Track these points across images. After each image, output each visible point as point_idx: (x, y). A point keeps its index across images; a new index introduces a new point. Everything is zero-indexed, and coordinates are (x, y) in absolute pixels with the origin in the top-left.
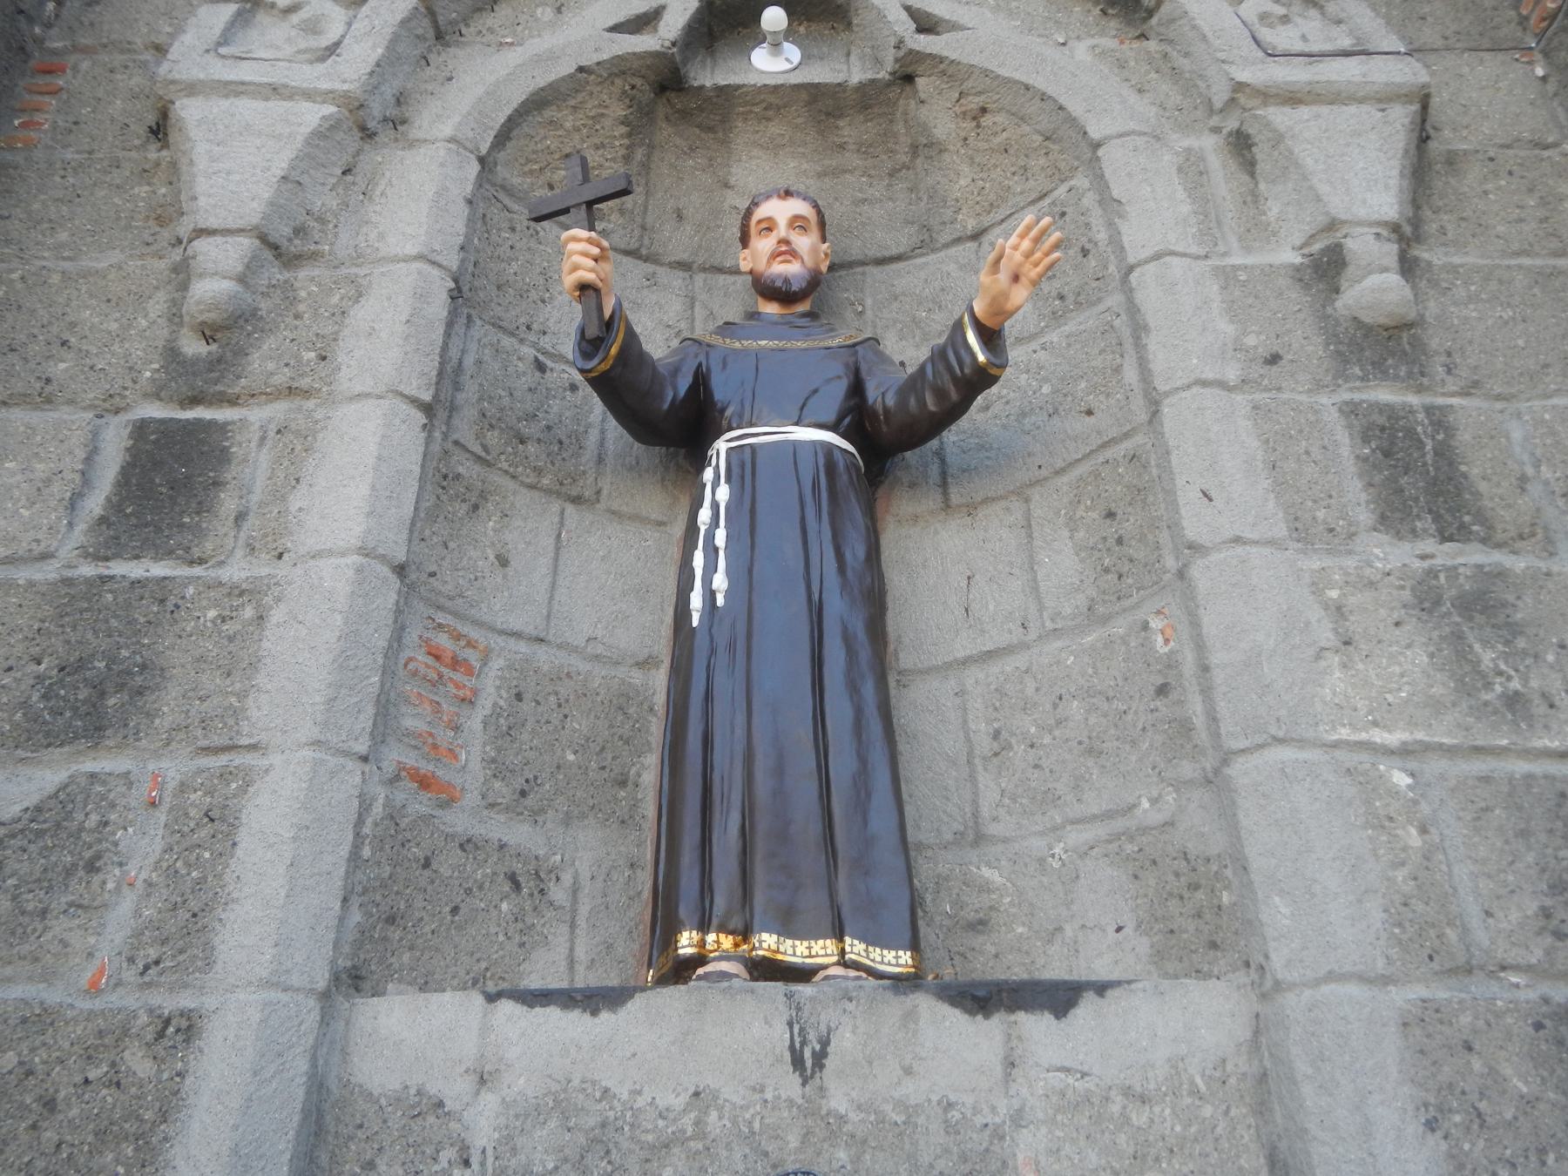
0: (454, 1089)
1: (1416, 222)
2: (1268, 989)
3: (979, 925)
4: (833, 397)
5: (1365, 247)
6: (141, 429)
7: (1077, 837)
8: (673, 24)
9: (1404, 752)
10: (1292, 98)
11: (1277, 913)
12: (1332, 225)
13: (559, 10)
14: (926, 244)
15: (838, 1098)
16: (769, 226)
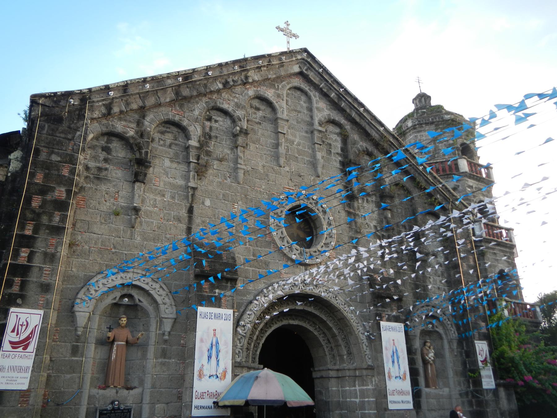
0: (96, 394)
1: (171, 330)
2: (143, 387)
3: (128, 381)
4: (126, 339)
5: (166, 333)
6: (73, 345)
7: (136, 376)
8: (118, 299)
9: (156, 375)
10: (166, 318)
11: (146, 385)
12: (165, 331)
13: (107, 296)
14: (135, 318)
15: (118, 395)
16: (122, 321)
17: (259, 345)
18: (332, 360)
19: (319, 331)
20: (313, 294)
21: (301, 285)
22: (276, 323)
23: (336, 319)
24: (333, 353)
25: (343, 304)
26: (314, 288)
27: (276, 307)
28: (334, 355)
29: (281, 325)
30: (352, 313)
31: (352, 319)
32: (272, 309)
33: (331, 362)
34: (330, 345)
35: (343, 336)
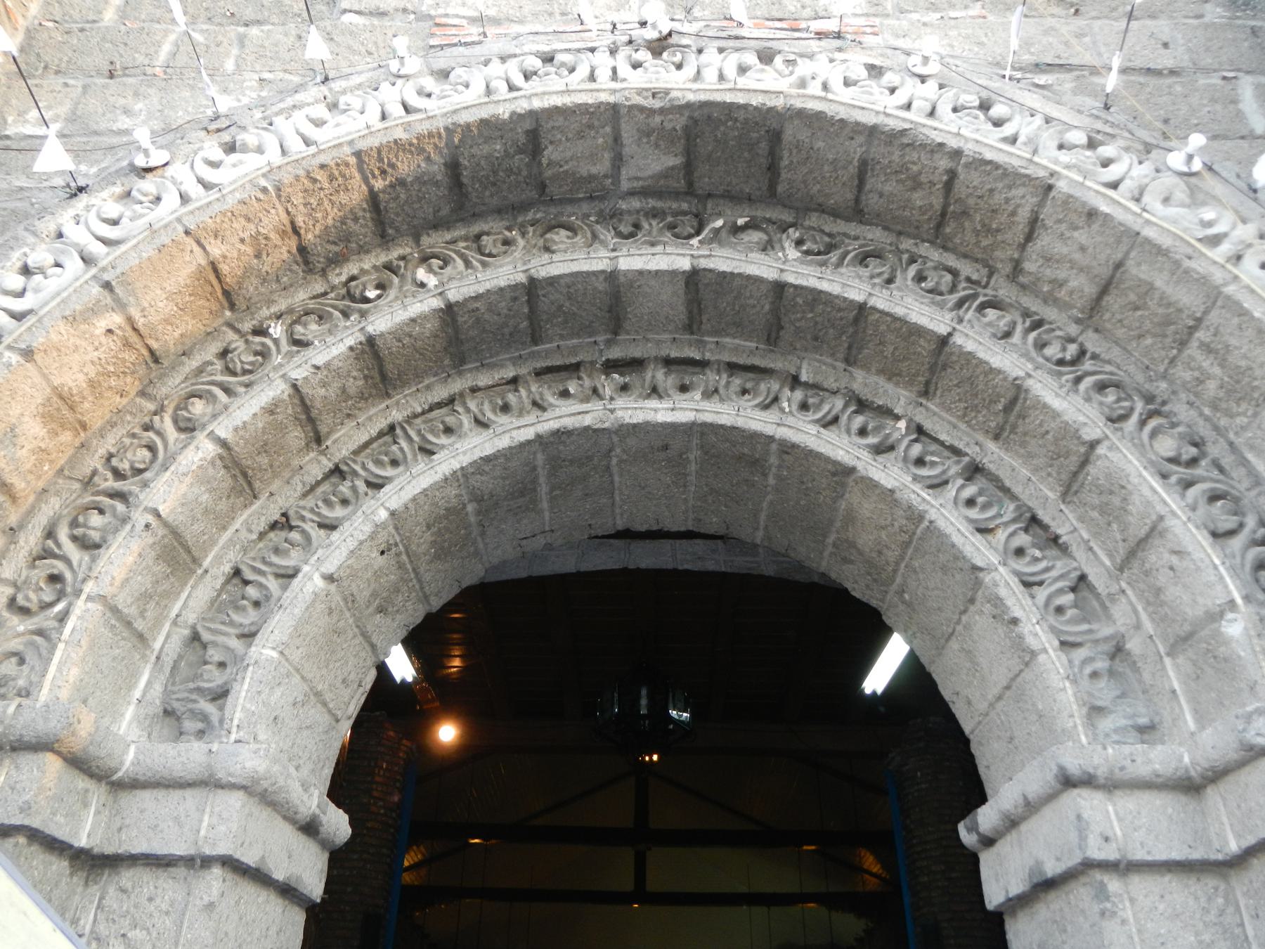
17: (285, 588)
18: (1105, 692)
19: (920, 462)
20: (729, 98)
21: (602, 61)
22: (481, 424)
23: (1050, 313)
24: (1106, 631)
25: (1079, 137)
26: (743, 70)
27: (421, 274)
28: (1118, 651)
29: (528, 434)
30: (1196, 198)
31: (1215, 241)
32: (381, 286)
33: (1095, 711)
34: (1060, 566)
35: (1167, 445)
